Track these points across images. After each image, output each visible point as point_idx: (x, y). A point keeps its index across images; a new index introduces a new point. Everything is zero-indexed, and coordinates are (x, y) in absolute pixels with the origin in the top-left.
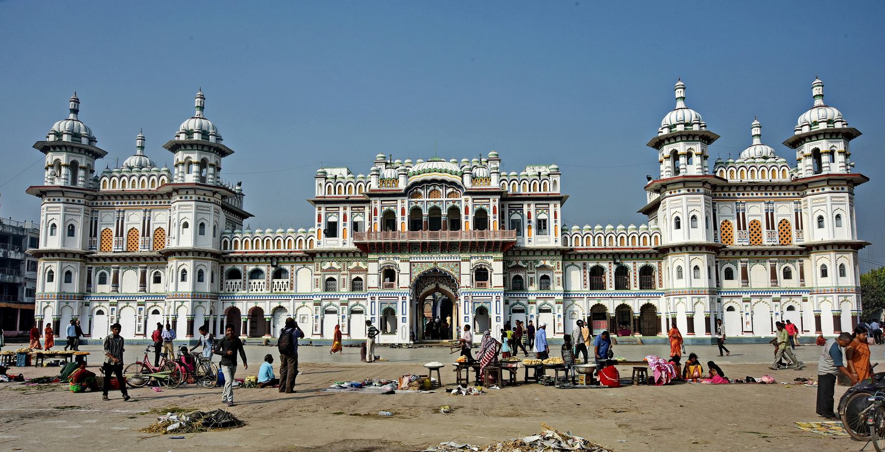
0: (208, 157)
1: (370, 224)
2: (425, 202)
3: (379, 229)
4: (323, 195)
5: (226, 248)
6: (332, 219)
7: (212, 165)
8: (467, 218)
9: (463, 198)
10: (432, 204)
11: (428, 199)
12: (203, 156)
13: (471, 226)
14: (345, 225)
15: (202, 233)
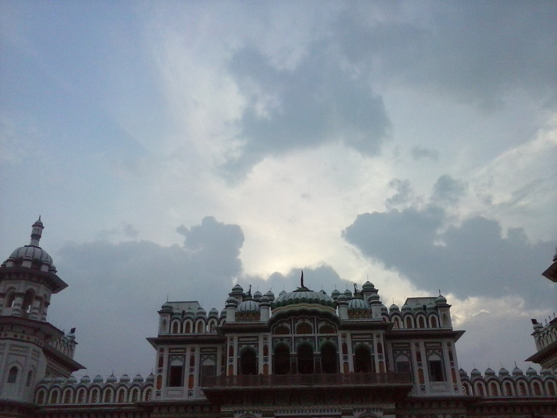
0: (35, 289)
1: (224, 369)
2: (293, 339)
3: (235, 373)
4: (166, 332)
5: (40, 401)
6: (177, 363)
7: (39, 298)
8: (345, 358)
9: (339, 333)
10: (301, 340)
11: (296, 335)
12: (29, 287)
13: (351, 369)
14: (192, 370)
15: (12, 380)
